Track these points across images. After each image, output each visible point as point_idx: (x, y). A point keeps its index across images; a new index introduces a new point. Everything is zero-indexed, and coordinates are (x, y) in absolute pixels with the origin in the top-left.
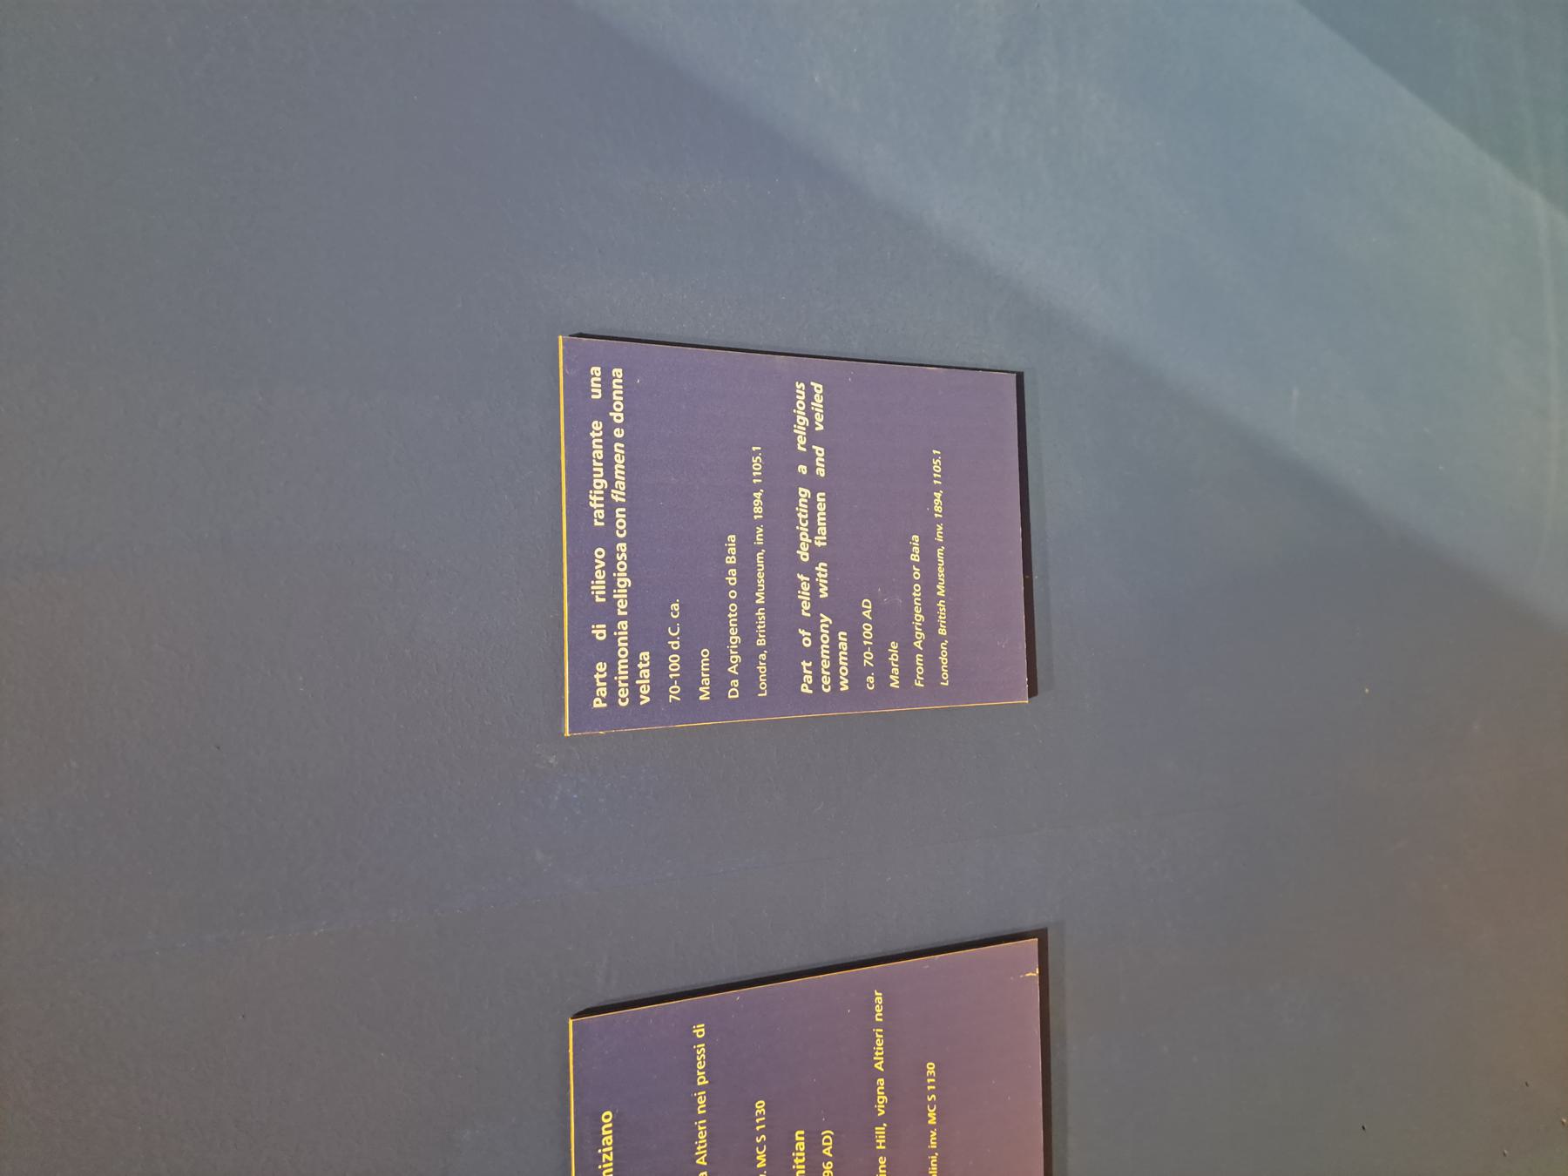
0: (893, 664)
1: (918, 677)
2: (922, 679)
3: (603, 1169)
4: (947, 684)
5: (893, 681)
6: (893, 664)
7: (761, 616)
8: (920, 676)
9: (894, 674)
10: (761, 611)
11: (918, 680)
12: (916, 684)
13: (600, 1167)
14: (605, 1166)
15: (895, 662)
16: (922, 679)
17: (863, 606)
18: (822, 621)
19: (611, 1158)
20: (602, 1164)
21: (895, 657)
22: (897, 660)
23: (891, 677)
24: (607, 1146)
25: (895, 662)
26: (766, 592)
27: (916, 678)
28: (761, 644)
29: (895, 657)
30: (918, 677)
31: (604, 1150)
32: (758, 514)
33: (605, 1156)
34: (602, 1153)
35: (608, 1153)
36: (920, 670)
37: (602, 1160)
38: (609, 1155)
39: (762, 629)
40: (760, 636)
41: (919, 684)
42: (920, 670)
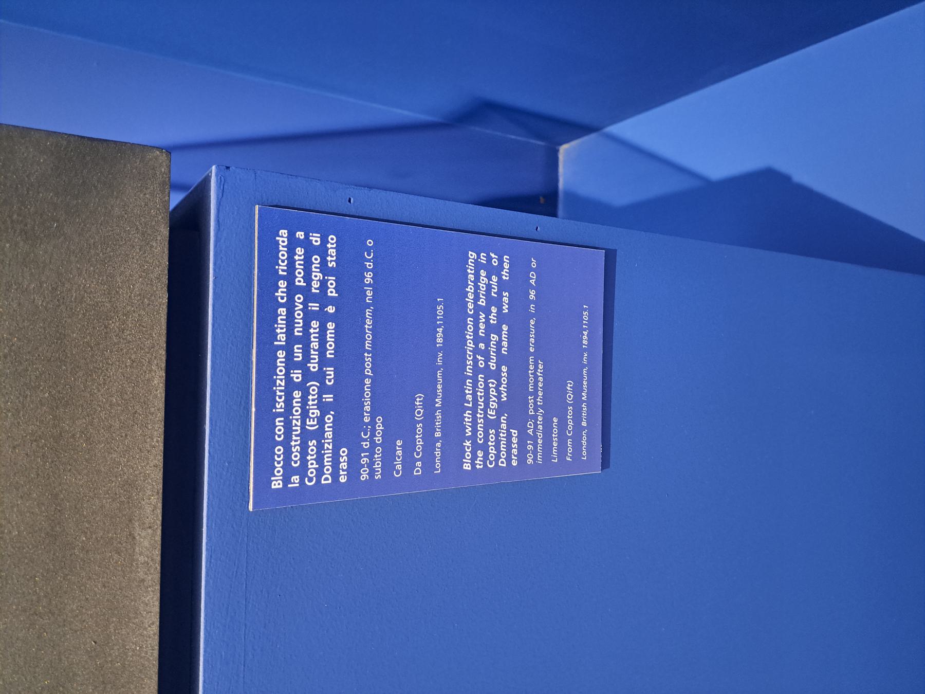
3: (325, 454)
4: (585, 459)
7: (438, 415)
10: (439, 412)
13: (323, 441)
14: (326, 452)
17: (528, 426)
18: (491, 400)
19: (330, 447)
20: (324, 450)
24: (328, 439)
26: (443, 399)
28: (438, 436)
31: (326, 441)
32: (440, 343)
33: (326, 445)
34: (325, 443)
35: (329, 443)
37: (324, 448)
38: (329, 445)
39: (438, 425)
40: (437, 430)
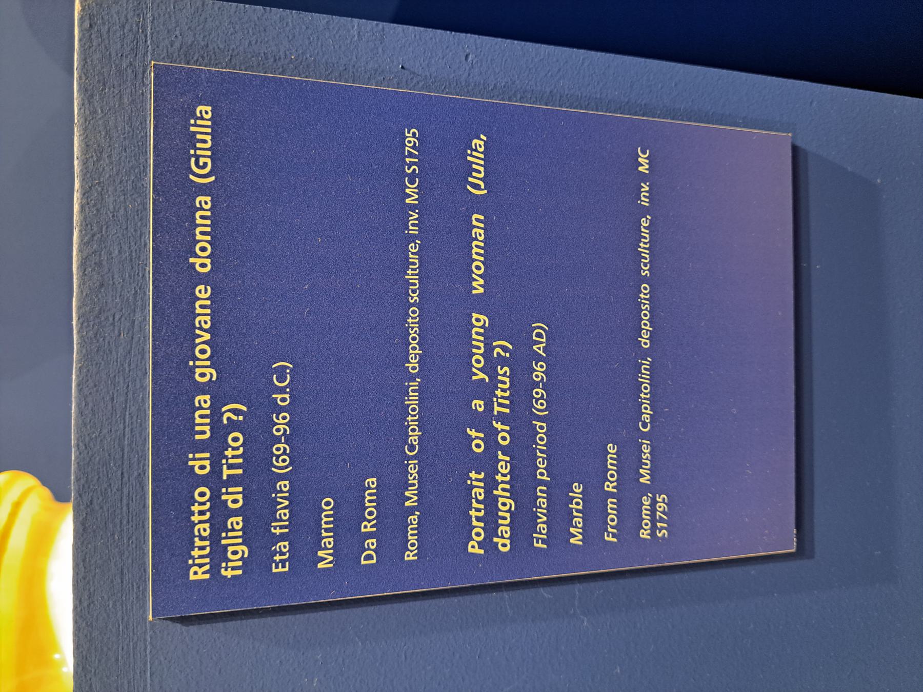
0: (575, 514)
1: (610, 529)
2: (615, 531)
5: (575, 536)
6: (575, 514)
8: (612, 527)
9: (576, 527)
11: (609, 533)
12: (606, 538)
15: (577, 511)
16: (615, 531)
21: (578, 504)
22: (580, 507)
23: (572, 530)
25: (577, 511)
27: (606, 530)
29: (578, 504)
30: (610, 529)
36: (612, 520)
41: (611, 539)
42: (612, 520)
